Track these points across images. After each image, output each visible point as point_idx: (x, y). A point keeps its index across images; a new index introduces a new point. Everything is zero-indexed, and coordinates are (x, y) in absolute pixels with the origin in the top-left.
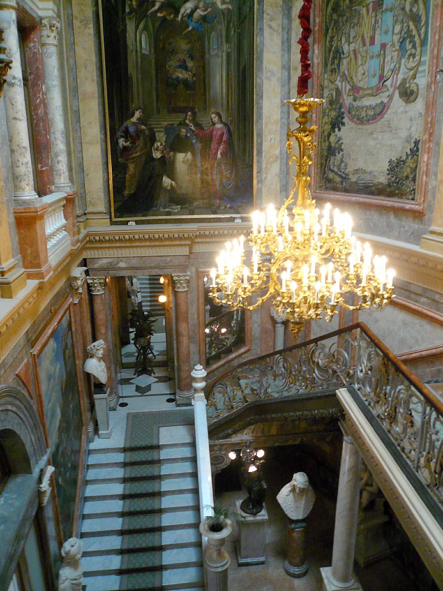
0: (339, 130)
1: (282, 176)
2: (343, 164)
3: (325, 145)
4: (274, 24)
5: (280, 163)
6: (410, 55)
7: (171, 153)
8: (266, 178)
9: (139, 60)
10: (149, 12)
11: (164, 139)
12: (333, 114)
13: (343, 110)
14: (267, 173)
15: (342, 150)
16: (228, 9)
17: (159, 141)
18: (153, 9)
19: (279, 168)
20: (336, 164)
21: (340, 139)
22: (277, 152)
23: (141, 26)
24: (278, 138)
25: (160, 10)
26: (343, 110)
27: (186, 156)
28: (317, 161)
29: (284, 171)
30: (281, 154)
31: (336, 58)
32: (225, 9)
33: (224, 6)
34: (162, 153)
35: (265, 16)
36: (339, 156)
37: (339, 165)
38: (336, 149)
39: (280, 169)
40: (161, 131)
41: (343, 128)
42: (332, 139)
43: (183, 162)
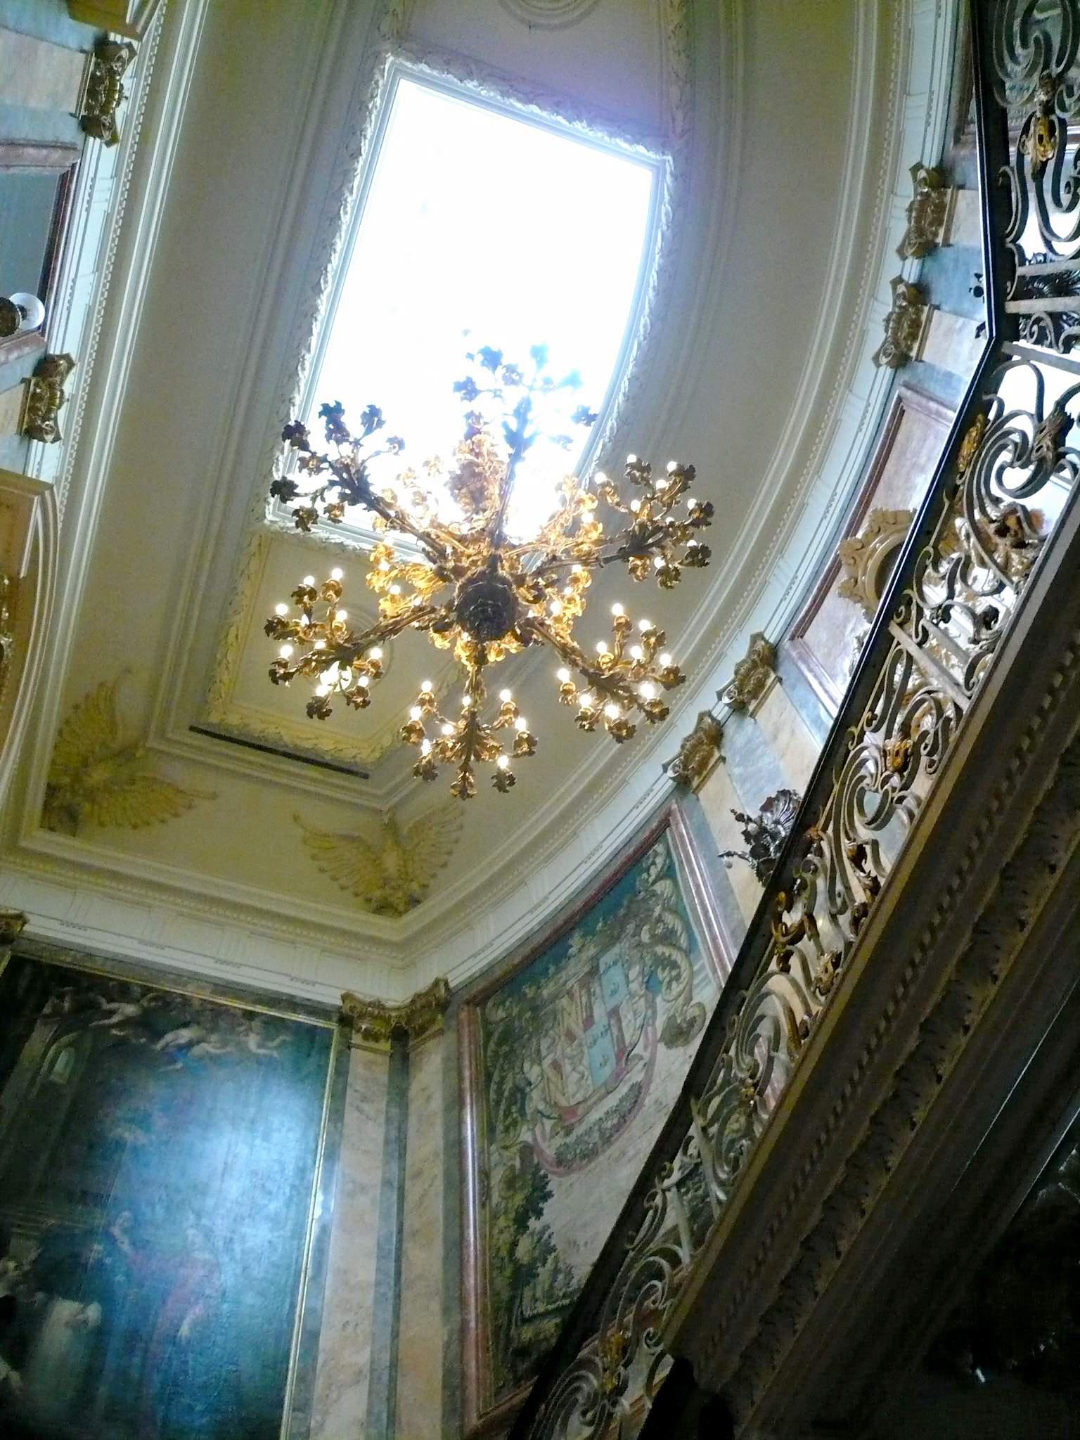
0: (539, 1213)
1: (373, 1431)
2: (561, 1277)
3: (501, 1282)
4: (366, 1107)
5: (370, 1392)
6: (670, 983)
7: (40, 1296)
8: (321, 1426)
9: (35, 1091)
10: (95, 1023)
11: (33, 1256)
12: (519, 1199)
13: (542, 1173)
14: (326, 1413)
15: (554, 1249)
16: (271, 1057)
17: (13, 1258)
18: (106, 1022)
19: (364, 1407)
20: (539, 1294)
21: (547, 1227)
22: (363, 1358)
23: (65, 1039)
24: (366, 1326)
25: (119, 1025)
26: (542, 1173)
27: (83, 1311)
28: (485, 1327)
29: (379, 1420)
30: (372, 1371)
31: (515, 1103)
32: (265, 1056)
33: (262, 1051)
34: (11, 1289)
35: (349, 1092)
36: (544, 1272)
37: (551, 1287)
38: (535, 1260)
39: (369, 1412)
40: (28, 1237)
41: (547, 1207)
42: (524, 1250)
43: (67, 1324)
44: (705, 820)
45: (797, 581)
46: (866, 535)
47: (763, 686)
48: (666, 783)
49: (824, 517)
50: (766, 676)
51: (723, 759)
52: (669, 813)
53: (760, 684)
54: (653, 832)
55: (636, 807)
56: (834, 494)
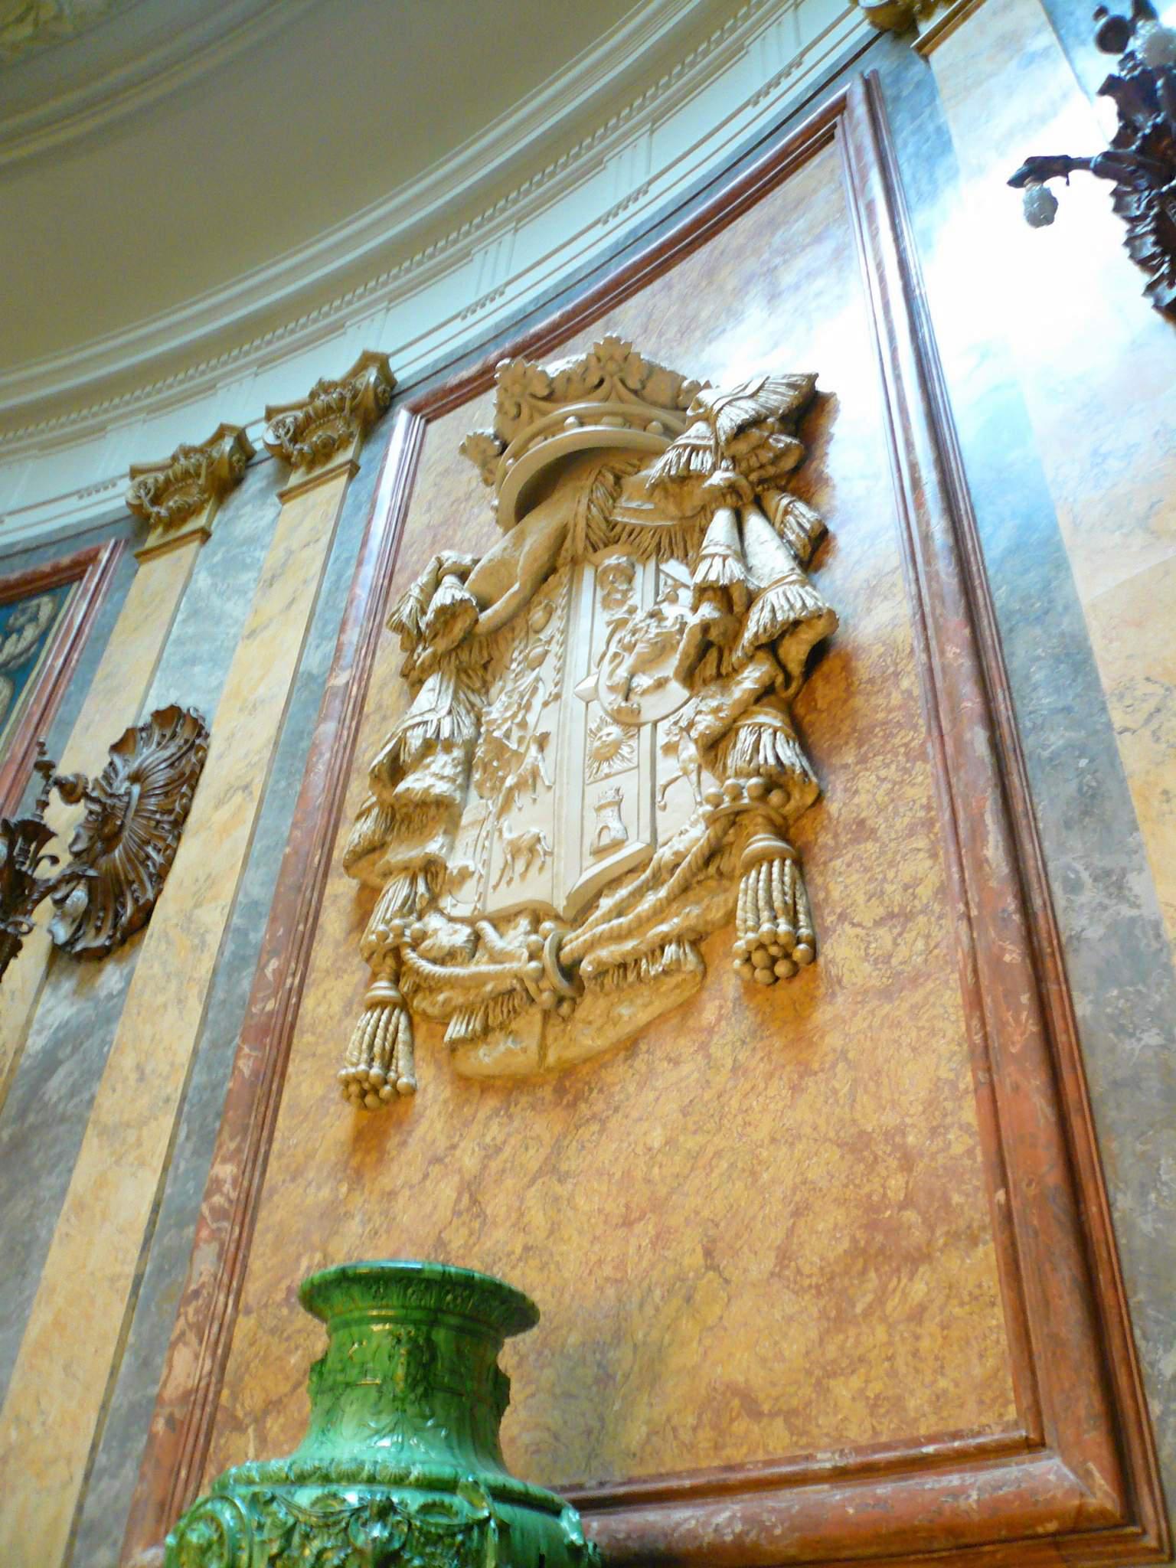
44: (111, 630)
45: (499, 301)
46: (567, 377)
47: (328, 457)
48: (118, 498)
49: (603, 220)
50: (343, 443)
51: (205, 535)
52: (92, 558)
53: (326, 451)
54: (57, 570)
55: (80, 494)
56: (643, 191)
